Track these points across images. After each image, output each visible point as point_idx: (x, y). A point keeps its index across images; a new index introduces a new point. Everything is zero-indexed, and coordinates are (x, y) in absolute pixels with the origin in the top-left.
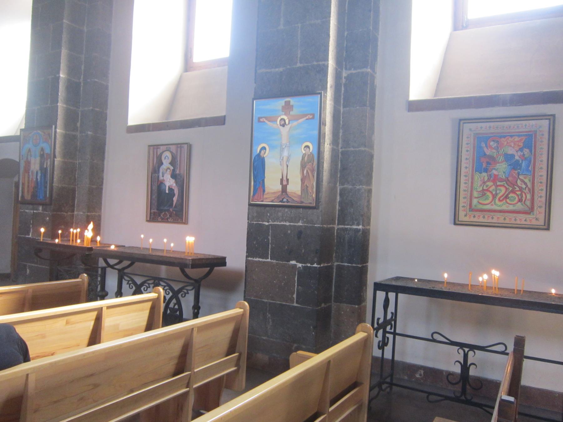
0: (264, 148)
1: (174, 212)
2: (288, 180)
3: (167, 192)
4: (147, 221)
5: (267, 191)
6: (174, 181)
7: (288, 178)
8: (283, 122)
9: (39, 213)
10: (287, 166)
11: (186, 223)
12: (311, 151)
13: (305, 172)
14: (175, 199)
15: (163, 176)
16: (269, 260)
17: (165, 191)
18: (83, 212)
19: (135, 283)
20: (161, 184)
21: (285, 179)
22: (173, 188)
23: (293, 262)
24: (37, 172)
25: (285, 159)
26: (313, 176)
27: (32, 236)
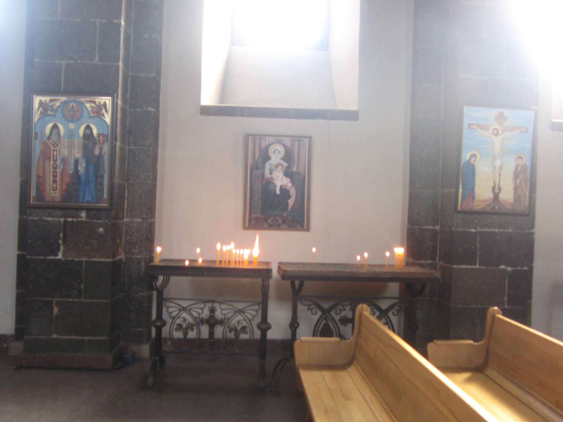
0: (474, 156)
1: (290, 218)
2: (500, 189)
3: (278, 192)
4: (245, 228)
5: (477, 198)
6: (288, 180)
7: (501, 186)
8: (495, 132)
9: (78, 222)
10: (500, 175)
11: (308, 229)
12: (524, 161)
13: (518, 181)
14: (291, 202)
15: (271, 173)
16: (477, 266)
17: (275, 191)
18: (142, 219)
19: (379, 309)
20: (268, 184)
21: (497, 187)
22: (288, 188)
23: (502, 267)
24: (76, 162)
25: (497, 168)
26: (526, 186)
27: (63, 255)
